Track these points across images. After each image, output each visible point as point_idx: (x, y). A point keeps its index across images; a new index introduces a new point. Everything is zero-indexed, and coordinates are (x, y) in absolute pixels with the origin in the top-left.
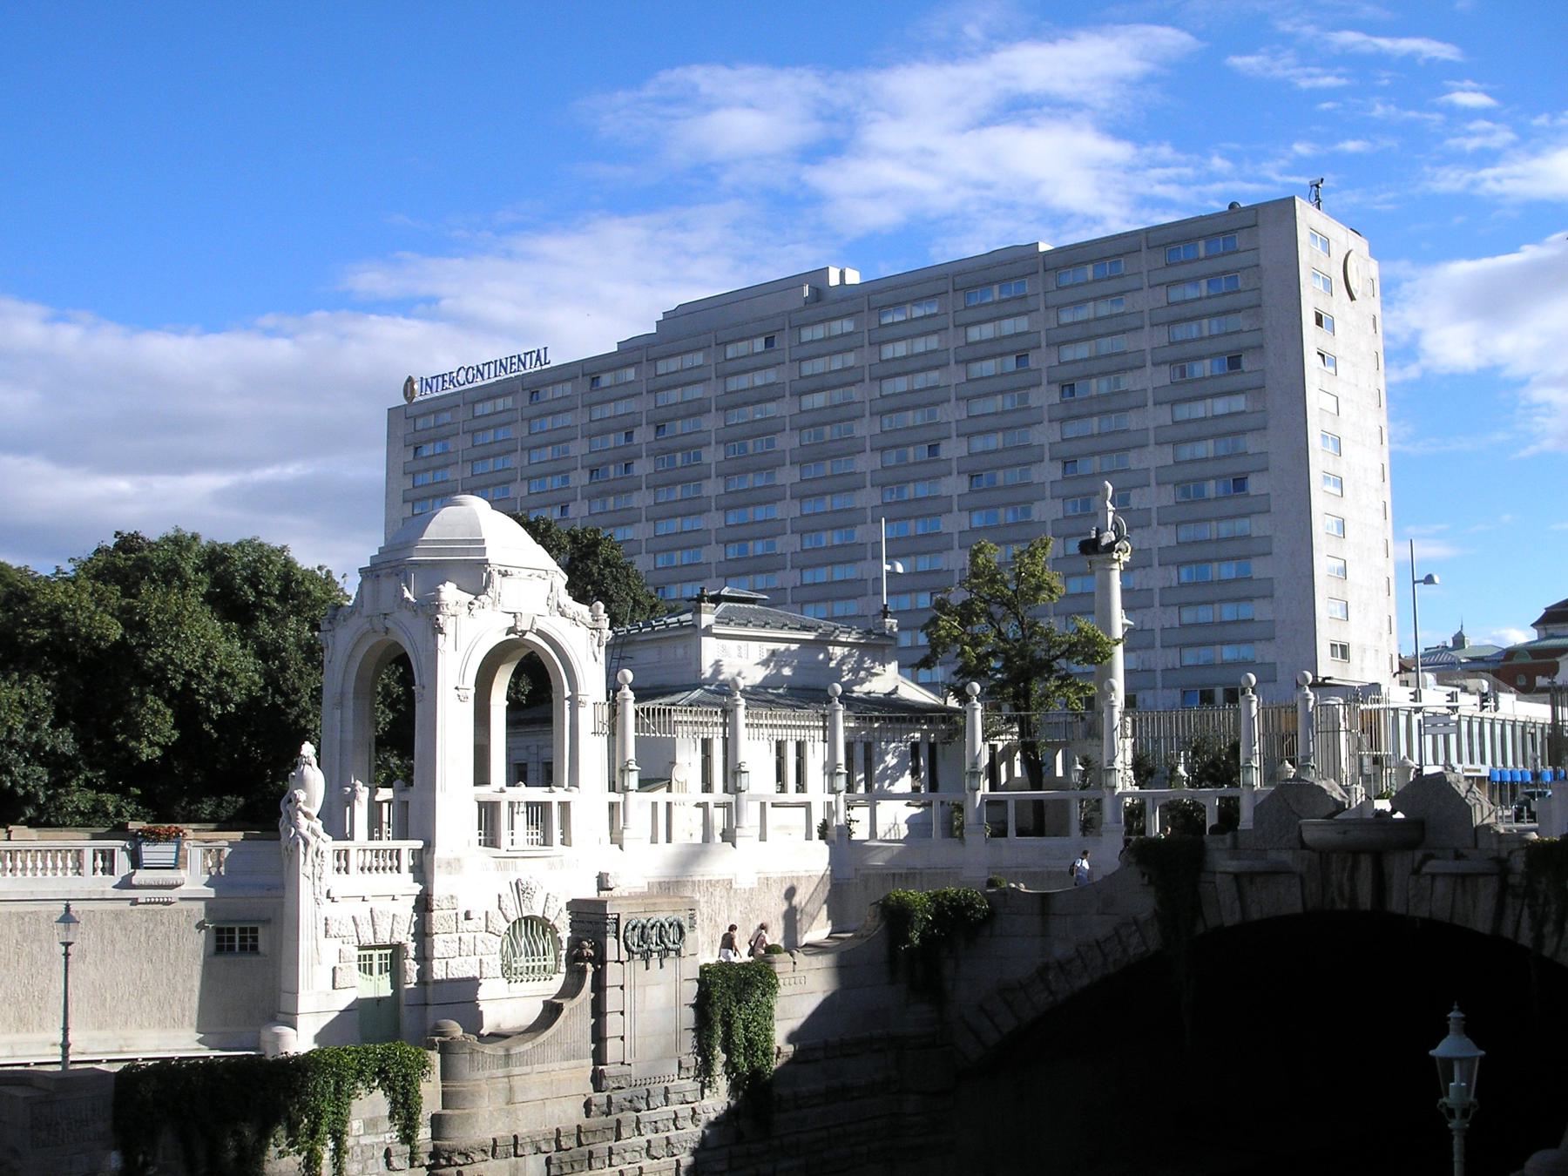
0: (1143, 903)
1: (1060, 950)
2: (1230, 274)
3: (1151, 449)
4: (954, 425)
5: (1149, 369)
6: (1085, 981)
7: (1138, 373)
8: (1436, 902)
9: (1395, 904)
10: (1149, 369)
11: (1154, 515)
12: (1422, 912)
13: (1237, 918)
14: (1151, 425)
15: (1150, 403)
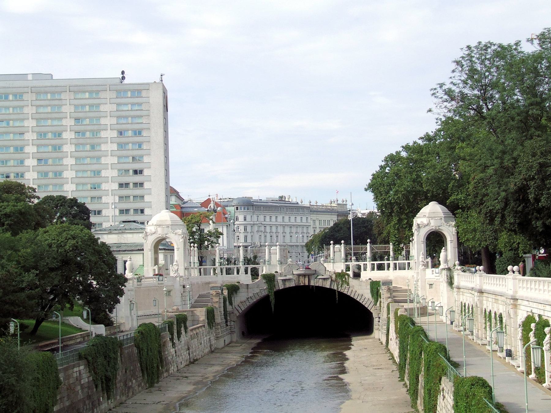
0: (265, 287)
1: (251, 295)
2: (140, 104)
3: (109, 157)
4: (31, 141)
5: (109, 131)
6: (255, 300)
7: (105, 131)
8: (320, 284)
9: (312, 283)
10: (109, 131)
11: (110, 179)
12: (317, 285)
13: (283, 288)
14: (110, 150)
15: (109, 142)
